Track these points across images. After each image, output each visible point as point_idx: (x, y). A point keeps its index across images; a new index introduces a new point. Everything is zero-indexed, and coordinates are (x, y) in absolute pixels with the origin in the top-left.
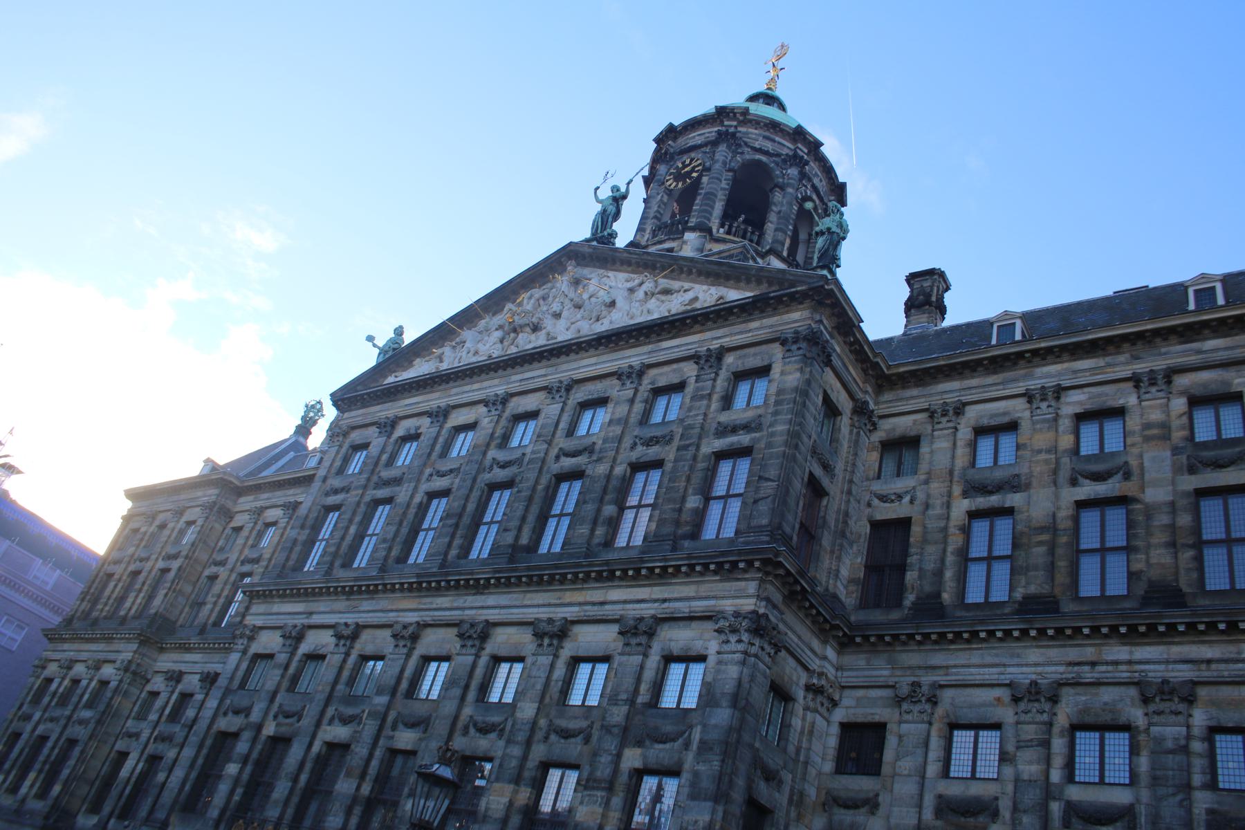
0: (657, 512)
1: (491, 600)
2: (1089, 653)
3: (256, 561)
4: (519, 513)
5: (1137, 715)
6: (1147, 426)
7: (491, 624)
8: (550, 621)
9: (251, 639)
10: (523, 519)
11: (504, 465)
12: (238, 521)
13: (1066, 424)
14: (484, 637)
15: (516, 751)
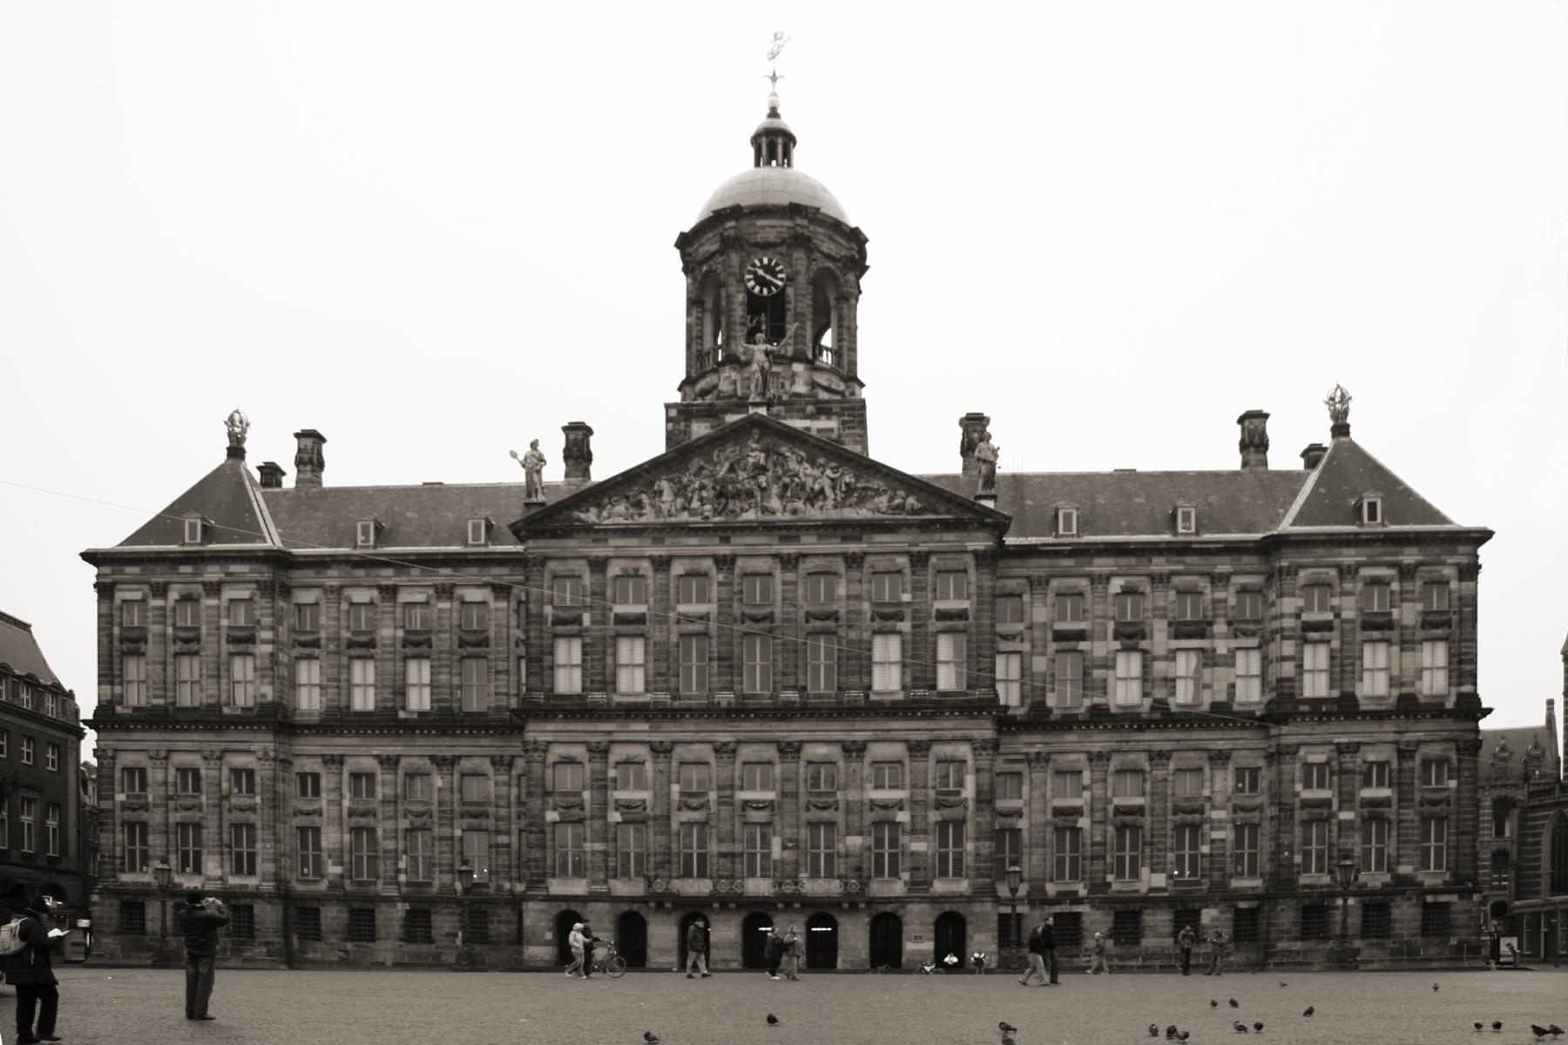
0: (909, 670)
1: (794, 726)
2: (1125, 736)
3: (371, 644)
4: (791, 662)
5: (1147, 767)
6: (1155, 609)
7: (802, 742)
8: (854, 742)
9: (545, 751)
10: (796, 666)
11: (756, 620)
12: (306, 597)
13: (1110, 599)
14: (798, 750)
15: (856, 818)
